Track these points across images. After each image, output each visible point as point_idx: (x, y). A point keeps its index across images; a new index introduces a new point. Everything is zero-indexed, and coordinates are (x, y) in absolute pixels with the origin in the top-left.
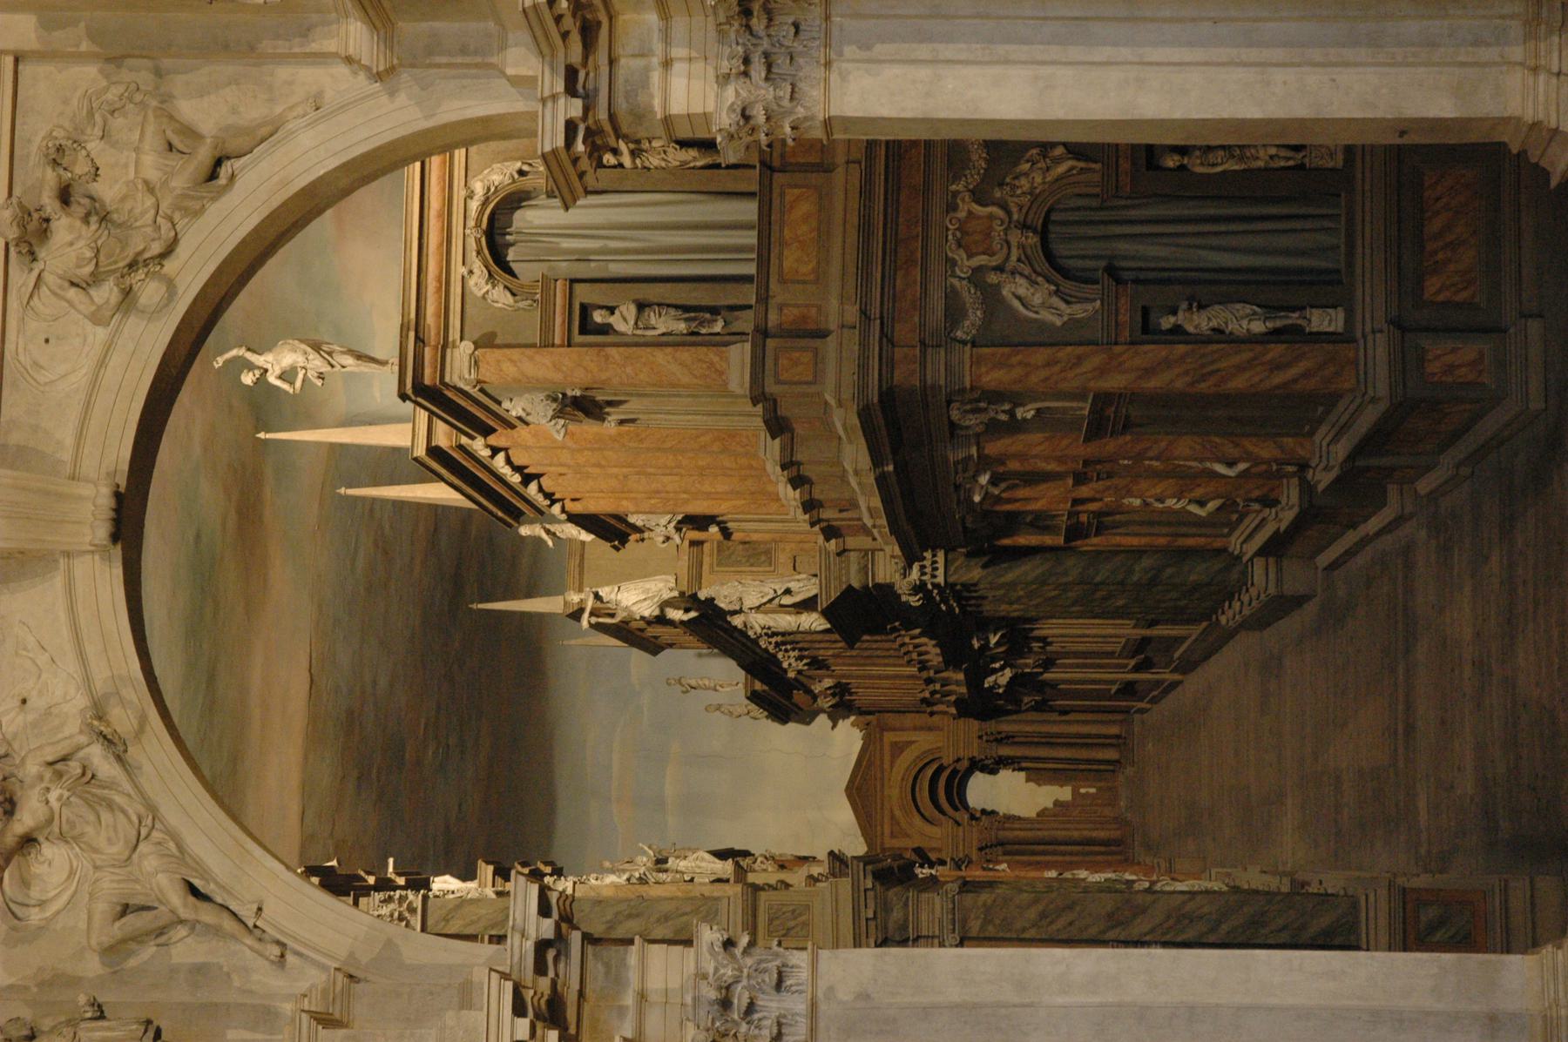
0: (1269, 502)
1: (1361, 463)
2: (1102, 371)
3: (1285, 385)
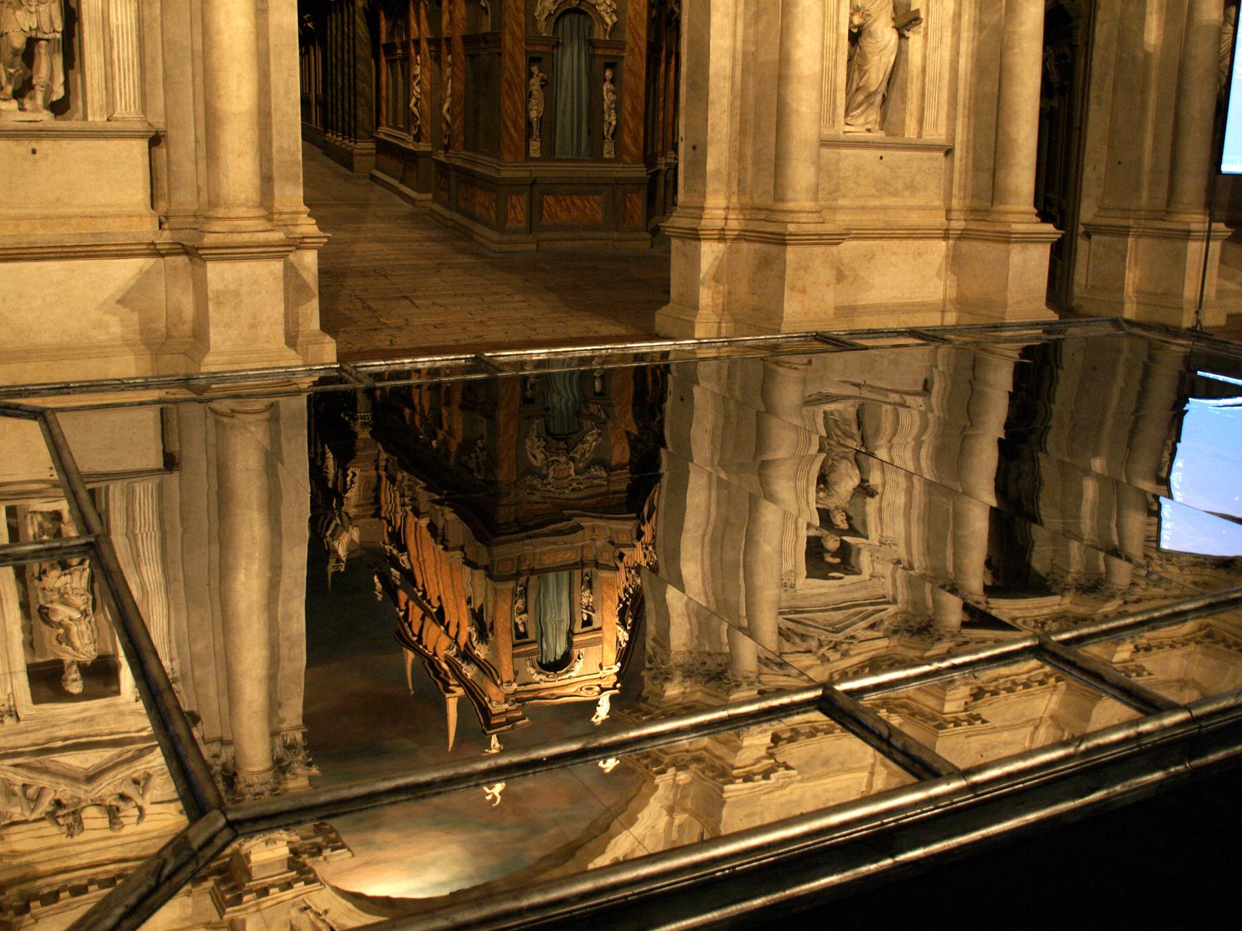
0: (417, 138)
1: (453, 174)
2: (513, 34)
3: (507, 127)
